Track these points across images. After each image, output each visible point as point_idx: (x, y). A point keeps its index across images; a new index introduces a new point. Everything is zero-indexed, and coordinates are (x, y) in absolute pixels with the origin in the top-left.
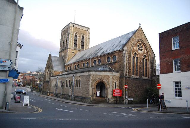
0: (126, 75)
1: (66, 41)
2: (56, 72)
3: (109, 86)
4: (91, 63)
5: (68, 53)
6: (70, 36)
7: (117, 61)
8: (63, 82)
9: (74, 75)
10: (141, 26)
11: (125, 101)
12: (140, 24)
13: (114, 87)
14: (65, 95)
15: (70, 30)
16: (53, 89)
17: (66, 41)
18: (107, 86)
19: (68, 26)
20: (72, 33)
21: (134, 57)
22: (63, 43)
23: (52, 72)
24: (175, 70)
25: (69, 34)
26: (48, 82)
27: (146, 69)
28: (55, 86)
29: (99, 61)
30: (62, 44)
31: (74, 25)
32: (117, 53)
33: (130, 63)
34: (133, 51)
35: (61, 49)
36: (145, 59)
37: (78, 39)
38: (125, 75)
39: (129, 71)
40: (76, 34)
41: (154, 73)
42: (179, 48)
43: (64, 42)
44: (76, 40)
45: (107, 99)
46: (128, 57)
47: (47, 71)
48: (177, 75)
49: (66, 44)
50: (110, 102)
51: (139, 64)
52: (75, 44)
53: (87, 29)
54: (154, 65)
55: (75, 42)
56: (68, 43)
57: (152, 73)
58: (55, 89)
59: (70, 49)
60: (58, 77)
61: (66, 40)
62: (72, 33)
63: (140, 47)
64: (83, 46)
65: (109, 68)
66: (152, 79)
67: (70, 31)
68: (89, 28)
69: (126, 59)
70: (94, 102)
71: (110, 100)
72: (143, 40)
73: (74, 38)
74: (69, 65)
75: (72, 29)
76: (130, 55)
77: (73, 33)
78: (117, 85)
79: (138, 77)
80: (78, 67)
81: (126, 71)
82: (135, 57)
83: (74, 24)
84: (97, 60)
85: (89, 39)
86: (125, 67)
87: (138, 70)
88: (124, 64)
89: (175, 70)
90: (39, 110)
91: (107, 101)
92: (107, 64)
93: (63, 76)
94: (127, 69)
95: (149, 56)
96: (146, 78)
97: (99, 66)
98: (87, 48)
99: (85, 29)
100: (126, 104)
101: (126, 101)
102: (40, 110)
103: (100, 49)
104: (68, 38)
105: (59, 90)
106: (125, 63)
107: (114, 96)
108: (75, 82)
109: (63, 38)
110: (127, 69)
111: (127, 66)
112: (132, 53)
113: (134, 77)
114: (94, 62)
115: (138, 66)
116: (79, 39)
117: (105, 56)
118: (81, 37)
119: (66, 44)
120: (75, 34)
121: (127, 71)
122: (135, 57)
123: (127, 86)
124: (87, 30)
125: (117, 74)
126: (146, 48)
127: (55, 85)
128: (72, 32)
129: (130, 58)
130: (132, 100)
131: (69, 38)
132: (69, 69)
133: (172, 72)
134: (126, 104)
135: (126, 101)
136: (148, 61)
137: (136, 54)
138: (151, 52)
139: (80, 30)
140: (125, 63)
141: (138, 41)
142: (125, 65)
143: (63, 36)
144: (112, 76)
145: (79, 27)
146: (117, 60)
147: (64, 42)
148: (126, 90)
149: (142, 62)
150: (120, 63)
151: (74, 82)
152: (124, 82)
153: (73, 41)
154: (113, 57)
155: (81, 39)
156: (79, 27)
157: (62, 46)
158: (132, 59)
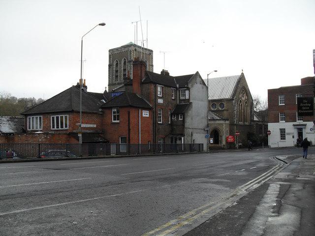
19: (126, 49)
48: (282, 124)
51: (242, 111)
68: (152, 51)
89: (281, 120)
126: (247, 95)
152: (235, 129)
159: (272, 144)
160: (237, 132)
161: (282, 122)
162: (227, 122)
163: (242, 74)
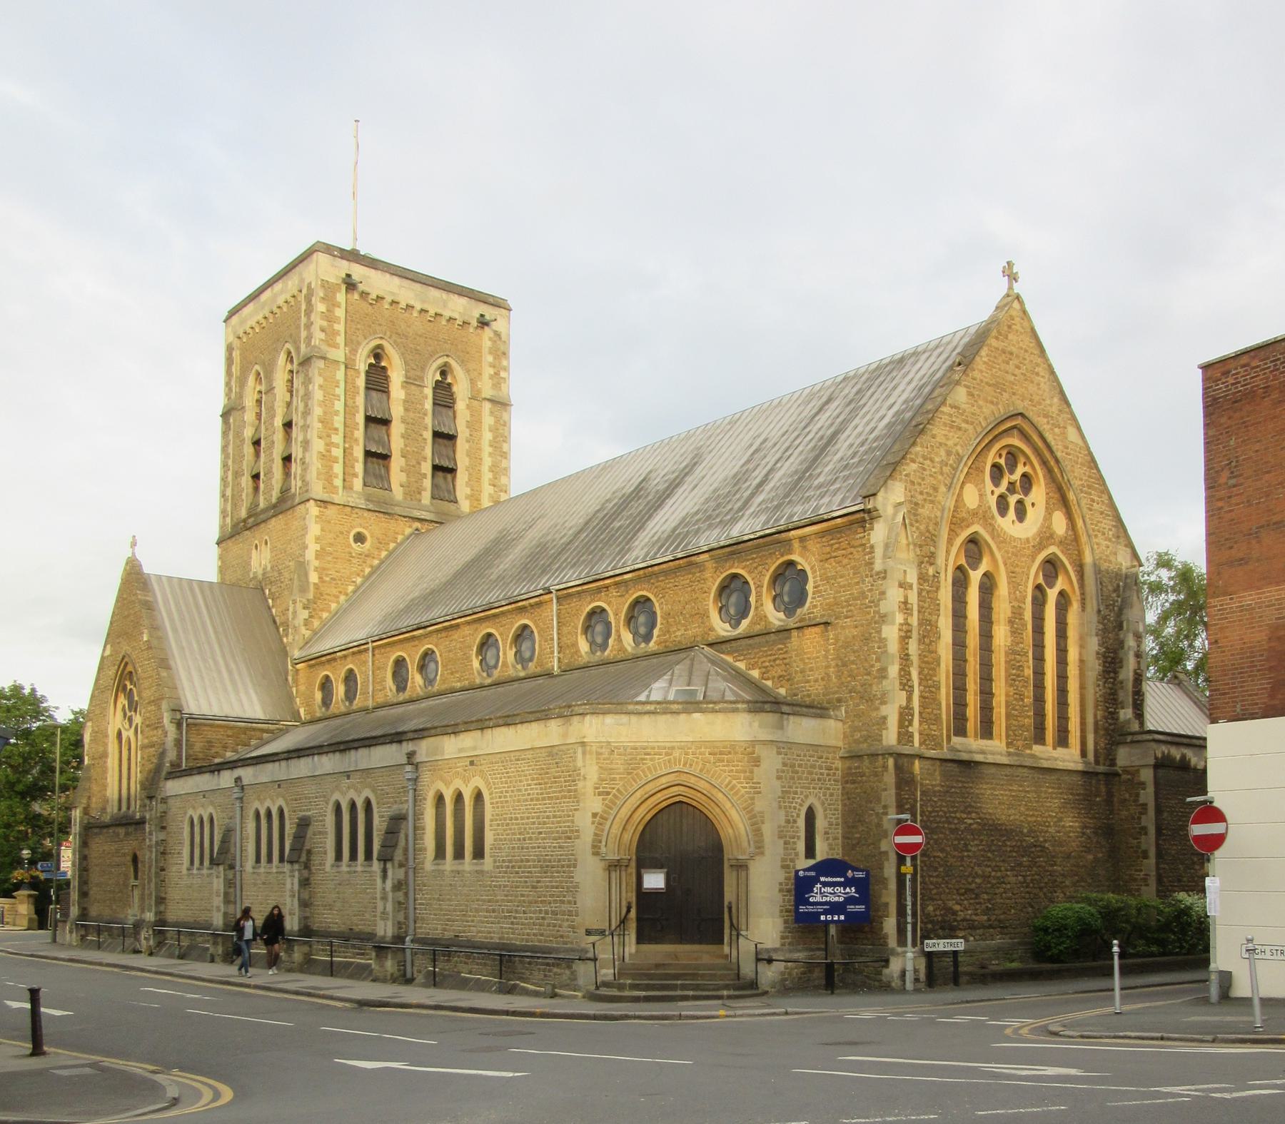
0: (905, 736)
1: (279, 436)
2: (211, 735)
3: (758, 832)
4: (559, 641)
5: (313, 548)
6: (318, 380)
7: (818, 615)
8: (304, 824)
9: (411, 755)
11: (895, 966)
13: (801, 846)
14: (327, 934)
15: (318, 322)
17: (288, 425)
19: (292, 283)
20: (339, 354)
21: (960, 582)
22: (249, 449)
23: (171, 730)
25: (306, 362)
28: (214, 862)
30: (239, 457)
31: (358, 271)
32: (813, 546)
33: (929, 633)
35: (235, 506)
36: (1052, 595)
37: (397, 411)
38: (890, 737)
39: (929, 699)
40: (377, 357)
41: (1126, 714)
43: (257, 443)
44: (378, 422)
45: (746, 947)
46: (912, 578)
49: (287, 459)
50: (769, 974)
51: (1001, 635)
52: (377, 458)
53: (478, 310)
54: (1131, 642)
55: (367, 437)
56: (306, 444)
57: (1112, 716)
59: (323, 503)
60: (247, 774)
61: (278, 422)
62: (339, 354)
63: (1011, 488)
64: (444, 470)
66: (1113, 763)
67: (318, 336)
68: (498, 304)
69: (894, 595)
70: (634, 987)
71: (770, 961)
72: (1042, 422)
73: (360, 400)
74: (328, 658)
75: (340, 313)
76: (932, 556)
77: (351, 344)
78: (820, 824)
79: (995, 749)
80: (429, 681)
83: (352, 256)
84: (616, 608)
85: (501, 404)
86: (893, 670)
87: (1000, 689)
88: (883, 642)
91: (747, 969)
92: (718, 644)
93: (302, 767)
97: (636, 658)
98: (487, 490)
99: (457, 307)
100: (909, 985)
101: (906, 961)
103: (637, 507)
104: (307, 396)
106: (891, 633)
107: (803, 921)
109: (249, 401)
110: (906, 685)
111: (905, 657)
112: (950, 541)
113: (965, 757)
114: (587, 628)
116: (408, 404)
117: (701, 567)
118: (429, 392)
119: (287, 459)
120: (363, 362)
121: (909, 699)
122: (975, 576)
124: (483, 323)
125: (828, 732)
127: (223, 857)
128: (340, 340)
130: (955, 953)
131: (318, 395)
134: (909, 985)
135: (906, 961)
137: (973, 541)
138: (1107, 524)
140: (891, 633)
141: (995, 433)
143: (242, 382)
144: (782, 747)
145: (407, 293)
146: (813, 605)
147: (257, 443)
148: (907, 868)
149: (1028, 615)
150: (847, 629)
151: (418, 816)
155: (428, 405)
156: (407, 293)
157: (237, 474)
160: (904, 830)
162: (803, 729)
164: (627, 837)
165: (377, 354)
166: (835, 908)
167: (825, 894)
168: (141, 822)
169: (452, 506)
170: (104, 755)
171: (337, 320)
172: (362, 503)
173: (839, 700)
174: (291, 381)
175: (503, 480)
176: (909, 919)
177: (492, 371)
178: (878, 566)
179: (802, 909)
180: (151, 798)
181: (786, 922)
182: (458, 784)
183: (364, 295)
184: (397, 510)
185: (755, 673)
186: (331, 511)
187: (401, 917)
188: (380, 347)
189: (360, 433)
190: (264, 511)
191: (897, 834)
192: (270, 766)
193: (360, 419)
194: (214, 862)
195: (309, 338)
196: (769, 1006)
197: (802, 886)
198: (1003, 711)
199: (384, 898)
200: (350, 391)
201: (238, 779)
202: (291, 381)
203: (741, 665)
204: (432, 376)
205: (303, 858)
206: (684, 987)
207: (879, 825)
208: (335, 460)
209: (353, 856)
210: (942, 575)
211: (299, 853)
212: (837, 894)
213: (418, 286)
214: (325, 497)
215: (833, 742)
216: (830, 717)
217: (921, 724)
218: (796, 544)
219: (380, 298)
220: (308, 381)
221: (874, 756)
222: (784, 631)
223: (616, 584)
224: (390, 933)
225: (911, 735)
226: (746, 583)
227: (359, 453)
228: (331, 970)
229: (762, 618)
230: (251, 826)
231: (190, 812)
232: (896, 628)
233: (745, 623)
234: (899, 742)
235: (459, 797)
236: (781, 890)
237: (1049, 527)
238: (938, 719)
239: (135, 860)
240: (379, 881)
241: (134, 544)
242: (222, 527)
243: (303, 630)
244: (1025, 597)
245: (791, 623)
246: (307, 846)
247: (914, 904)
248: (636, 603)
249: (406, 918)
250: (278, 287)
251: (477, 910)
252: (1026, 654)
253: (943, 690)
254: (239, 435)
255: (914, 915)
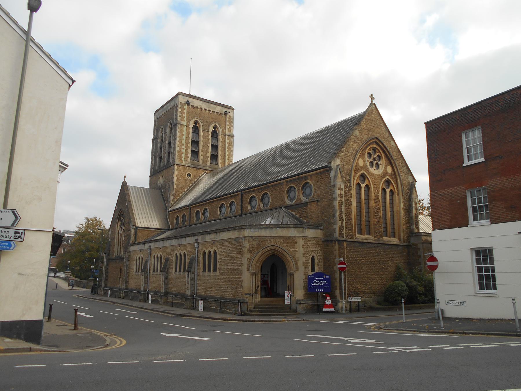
0: (341, 234)
1: (167, 146)
3: (297, 264)
5: (175, 178)
6: (178, 130)
8: (167, 260)
9: (197, 240)
10: (374, 101)
12: (372, 97)
13: (310, 268)
15: (179, 114)
16: (136, 280)
17: (170, 143)
18: (291, 266)
19: (172, 103)
20: (185, 123)
22: (159, 150)
24: (475, 219)
25: (175, 125)
26: (120, 259)
27: (393, 216)
28: (142, 271)
29: (266, 200)
33: (349, 203)
34: (357, 171)
35: (155, 166)
36: (388, 191)
39: (349, 223)
42: (483, 160)
43: (161, 148)
44: (195, 143)
46: (343, 187)
47: (118, 229)
48: (481, 233)
49: (169, 153)
50: (300, 308)
51: (372, 203)
52: (195, 153)
53: (225, 110)
54: (414, 205)
56: (174, 148)
58: (143, 278)
59: (178, 165)
60: (152, 245)
61: (167, 142)
62: (185, 123)
63: (374, 159)
65: (294, 217)
67: (179, 118)
68: (231, 108)
69: (338, 192)
70: (259, 311)
71: (300, 304)
73: (190, 136)
75: (185, 111)
76: (349, 181)
77: (189, 120)
78: (316, 261)
79: (370, 238)
81: (339, 223)
82: (363, 186)
84: (258, 196)
85: (232, 136)
88: (334, 206)
89: (475, 219)
90: (116, 342)
92: (287, 207)
93: (167, 243)
94: (341, 219)
95: (399, 181)
96: (394, 241)
98: (227, 161)
99: (218, 109)
101: (342, 304)
102: (119, 342)
104: (175, 135)
105: (157, 282)
107: (310, 292)
108: (201, 257)
109: (160, 136)
110: (341, 219)
111: (341, 210)
112: (355, 176)
113: (361, 240)
114: (250, 202)
115: (372, 211)
118: (210, 133)
119: (169, 153)
122: (363, 186)
123: (344, 264)
124: (226, 114)
126: (390, 161)
127: (144, 269)
128: (185, 119)
129: (348, 188)
131: (178, 134)
132: (180, 222)
133: (464, 223)
136: (396, 194)
137: (363, 176)
138: (405, 169)
139: (207, 114)
140: (337, 203)
142: (337, 208)
147: (161, 148)
149: (380, 197)
152: (337, 253)
153: (187, 143)
154: (303, 188)
155: (210, 137)
156: (204, 106)
157: (155, 157)
158: (353, 192)
159: (449, 303)
160: (342, 263)
161: (479, 222)
162: (310, 233)
163: (373, 110)
164: (258, 265)
165: (196, 123)
166: (320, 287)
167: (317, 283)
168: (123, 259)
169: (216, 166)
170: (114, 238)
171: (184, 113)
172: (190, 165)
173: (322, 224)
174: (171, 130)
175: (231, 158)
176: (343, 291)
177: (228, 127)
178: (332, 184)
179: (310, 287)
180: (126, 251)
181: (305, 291)
182: (210, 249)
183: (193, 106)
184: (200, 167)
185: (298, 216)
186: (181, 168)
187: (193, 289)
188: (196, 121)
189: (190, 145)
190: (162, 167)
191: (339, 265)
192: (158, 243)
193: (190, 141)
194: (142, 271)
195: (176, 118)
196: (299, 318)
197: (309, 281)
198: (373, 226)
199: (188, 283)
200: (188, 133)
201: (150, 246)
202: (171, 130)
203: (294, 213)
204: (211, 128)
205: (166, 271)
206: (274, 312)
207: (334, 262)
208: (182, 153)
209: (180, 270)
210: (352, 185)
211: (165, 269)
212: (321, 283)
213: (207, 104)
214: (179, 163)
215: (320, 237)
216: (318, 229)
217: (346, 230)
218: (309, 177)
219: (197, 107)
220: (176, 131)
221: (332, 241)
222: (306, 204)
223: (258, 189)
224: (189, 294)
225: (343, 234)
226: (295, 188)
227: (189, 151)
228: (173, 305)
229: (299, 199)
230: (153, 260)
231: (136, 256)
232: (338, 202)
233: (295, 201)
234: (339, 236)
235: (210, 252)
236: (304, 282)
237: (386, 171)
238: (352, 229)
239: (121, 269)
240: (187, 278)
241: (125, 177)
242: (151, 172)
243: (171, 202)
244: (379, 192)
245: (308, 200)
246: (168, 267)
247: (345, 286)
248: (264, 195)
249: (194, 289)
250: (168, 104)
251: (214, 287)
252: (380, 209)
253: (353, 220)
254: (156, 146)
255: (345, 289)
